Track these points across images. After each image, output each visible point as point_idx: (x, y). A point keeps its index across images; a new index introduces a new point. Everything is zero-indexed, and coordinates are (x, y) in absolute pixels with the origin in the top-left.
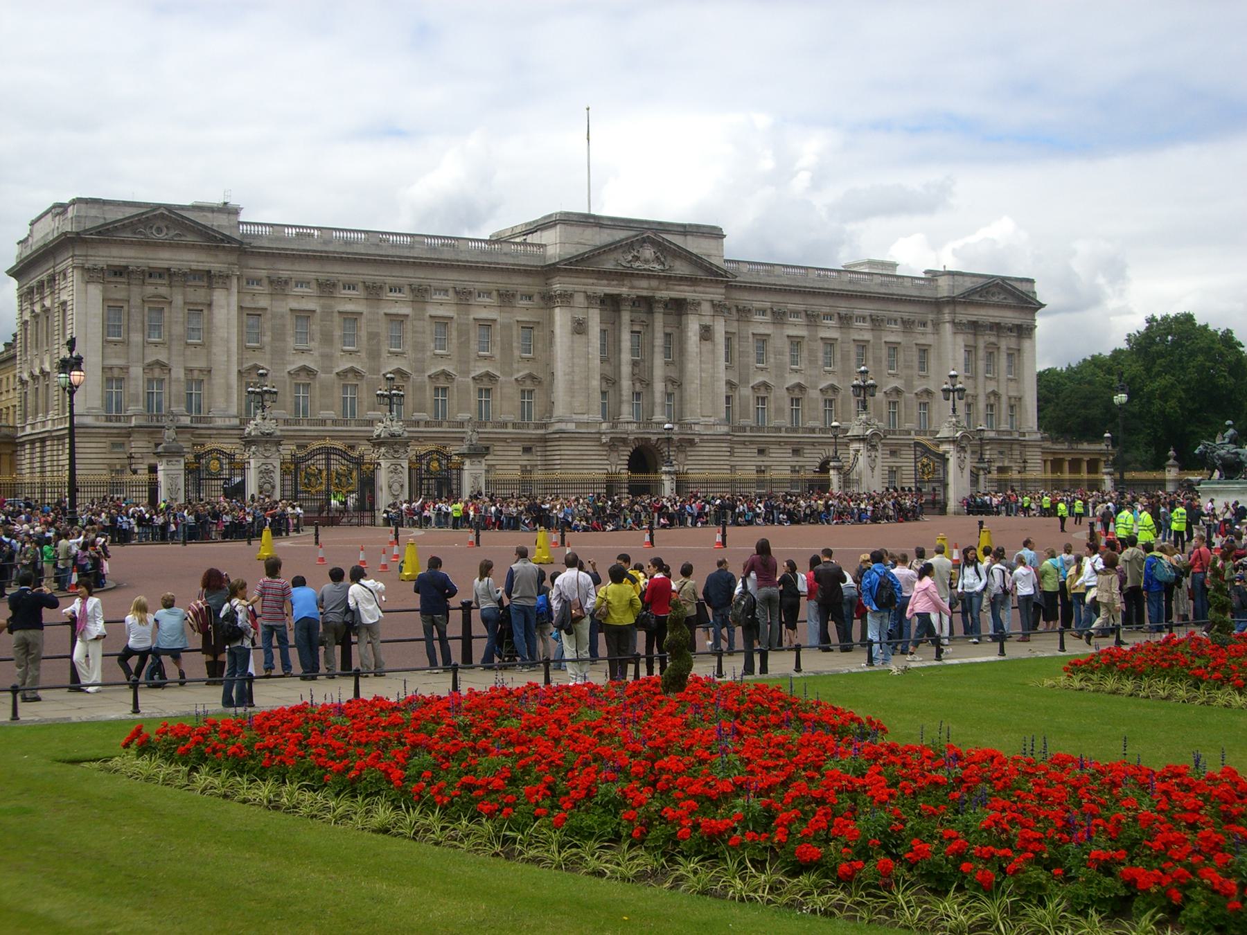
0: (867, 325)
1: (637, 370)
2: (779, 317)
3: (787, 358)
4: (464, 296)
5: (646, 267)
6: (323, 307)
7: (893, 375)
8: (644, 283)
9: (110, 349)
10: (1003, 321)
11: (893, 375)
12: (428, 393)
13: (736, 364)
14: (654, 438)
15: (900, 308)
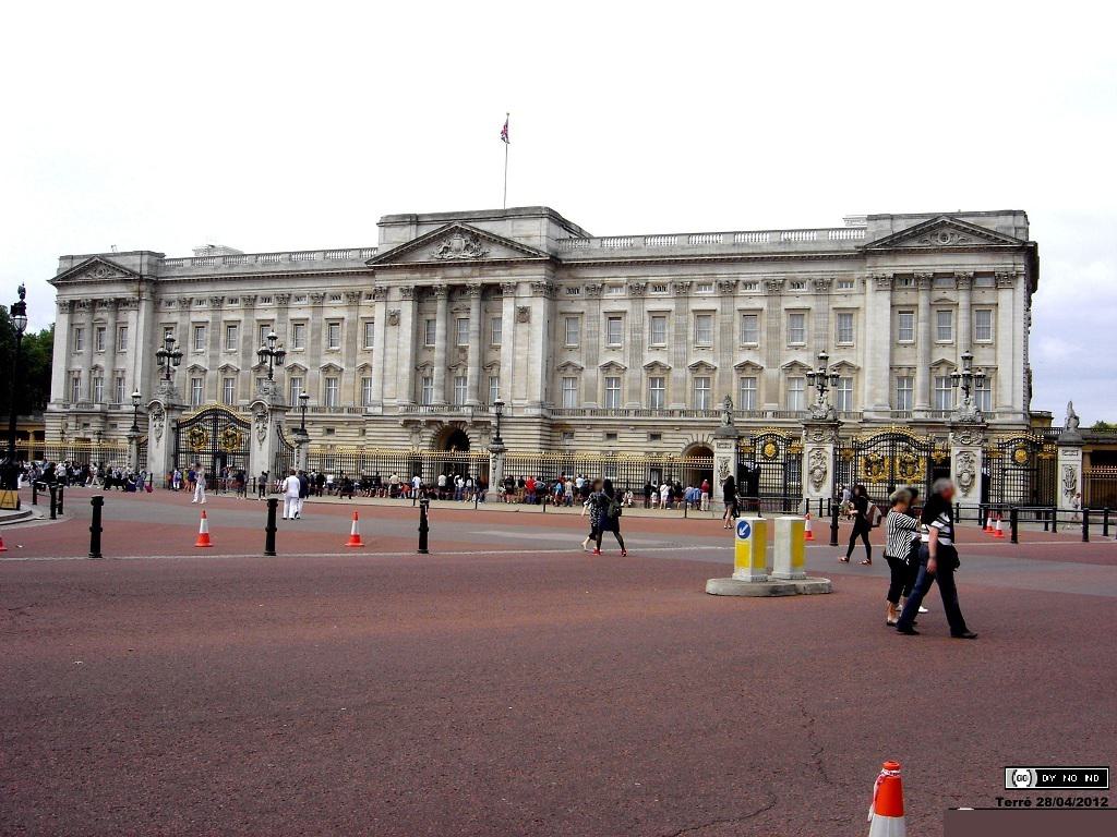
0: (757, 290)
1: (462, 356)
2: (638, 291)
3: (646, 336)
4: (318, 300)
5: (458, 256)
6: (213, 318)
7: (797, 348)
8: (456, 272)
9: (76, 358)
10: (959, 270)
11: (797, 348)
12: (286, 384)
13: (584, 345)
14: (446, 420)
15: (811, 267)
